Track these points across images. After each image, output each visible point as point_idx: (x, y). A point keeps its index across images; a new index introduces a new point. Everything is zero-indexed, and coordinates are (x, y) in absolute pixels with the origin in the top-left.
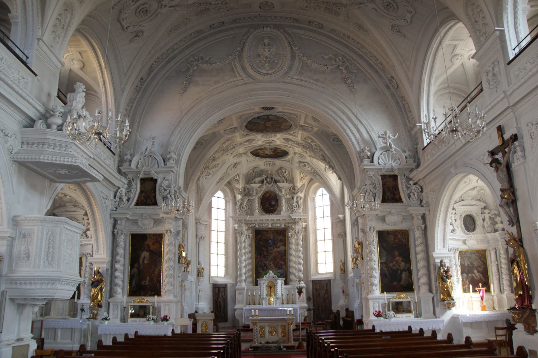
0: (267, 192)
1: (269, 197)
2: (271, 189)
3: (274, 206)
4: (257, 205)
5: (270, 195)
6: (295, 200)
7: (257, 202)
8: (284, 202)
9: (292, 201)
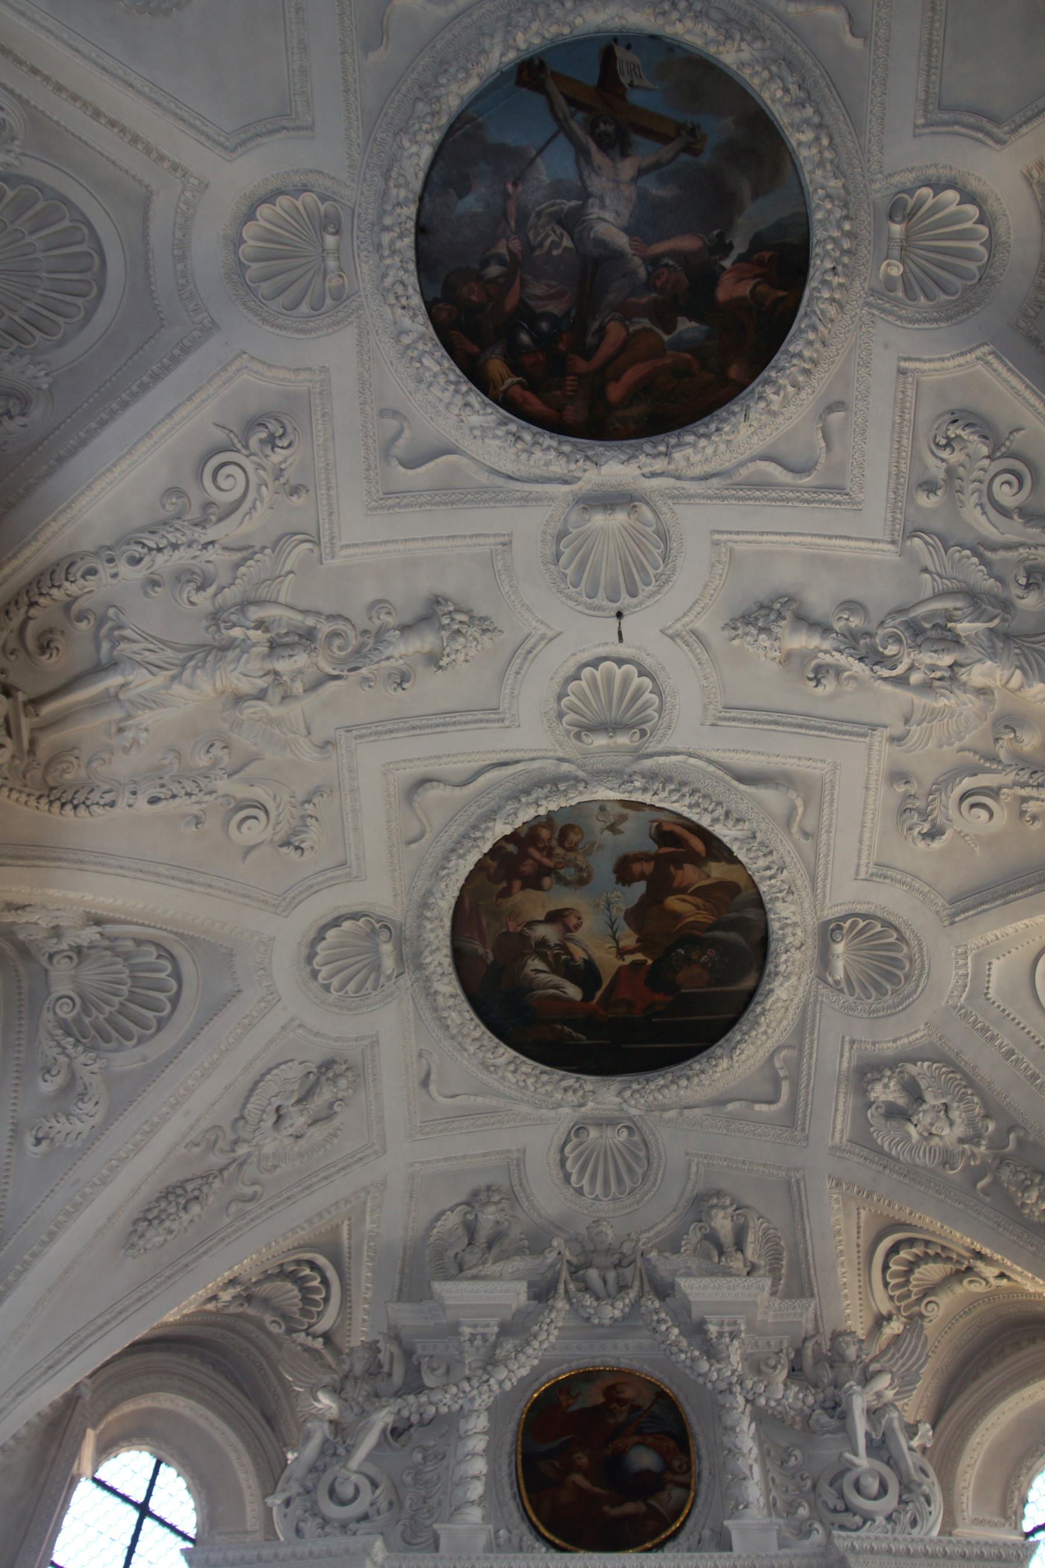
0: (587, 1376)
1: (596, 1409)
2: (624, 1353)
3: (648, 1484)
4: (479, 1466)
5: (611, 1393)
6: (861, 1426)
7: (479, 1444)
8: (746, 1438)
9: (829, 1450)
